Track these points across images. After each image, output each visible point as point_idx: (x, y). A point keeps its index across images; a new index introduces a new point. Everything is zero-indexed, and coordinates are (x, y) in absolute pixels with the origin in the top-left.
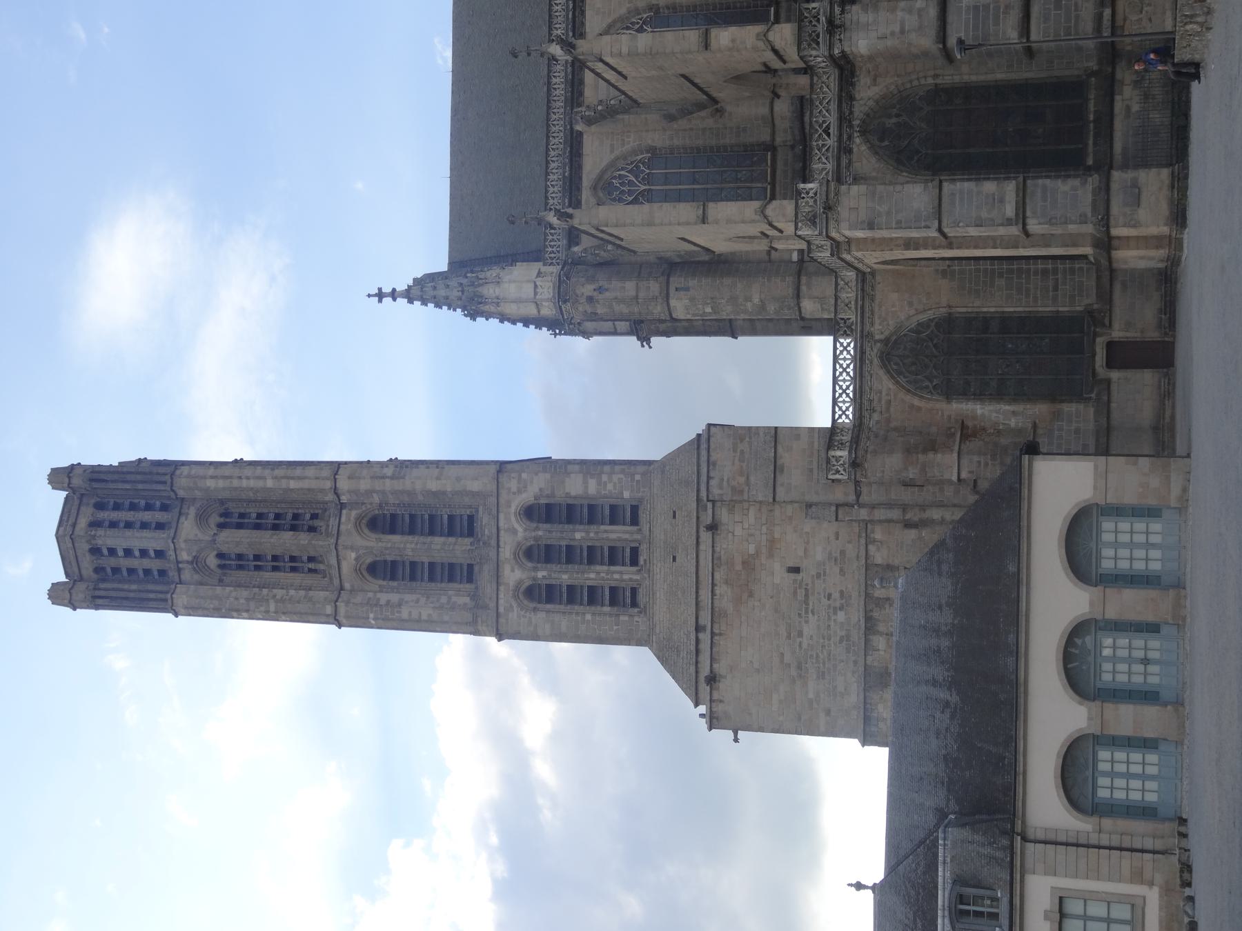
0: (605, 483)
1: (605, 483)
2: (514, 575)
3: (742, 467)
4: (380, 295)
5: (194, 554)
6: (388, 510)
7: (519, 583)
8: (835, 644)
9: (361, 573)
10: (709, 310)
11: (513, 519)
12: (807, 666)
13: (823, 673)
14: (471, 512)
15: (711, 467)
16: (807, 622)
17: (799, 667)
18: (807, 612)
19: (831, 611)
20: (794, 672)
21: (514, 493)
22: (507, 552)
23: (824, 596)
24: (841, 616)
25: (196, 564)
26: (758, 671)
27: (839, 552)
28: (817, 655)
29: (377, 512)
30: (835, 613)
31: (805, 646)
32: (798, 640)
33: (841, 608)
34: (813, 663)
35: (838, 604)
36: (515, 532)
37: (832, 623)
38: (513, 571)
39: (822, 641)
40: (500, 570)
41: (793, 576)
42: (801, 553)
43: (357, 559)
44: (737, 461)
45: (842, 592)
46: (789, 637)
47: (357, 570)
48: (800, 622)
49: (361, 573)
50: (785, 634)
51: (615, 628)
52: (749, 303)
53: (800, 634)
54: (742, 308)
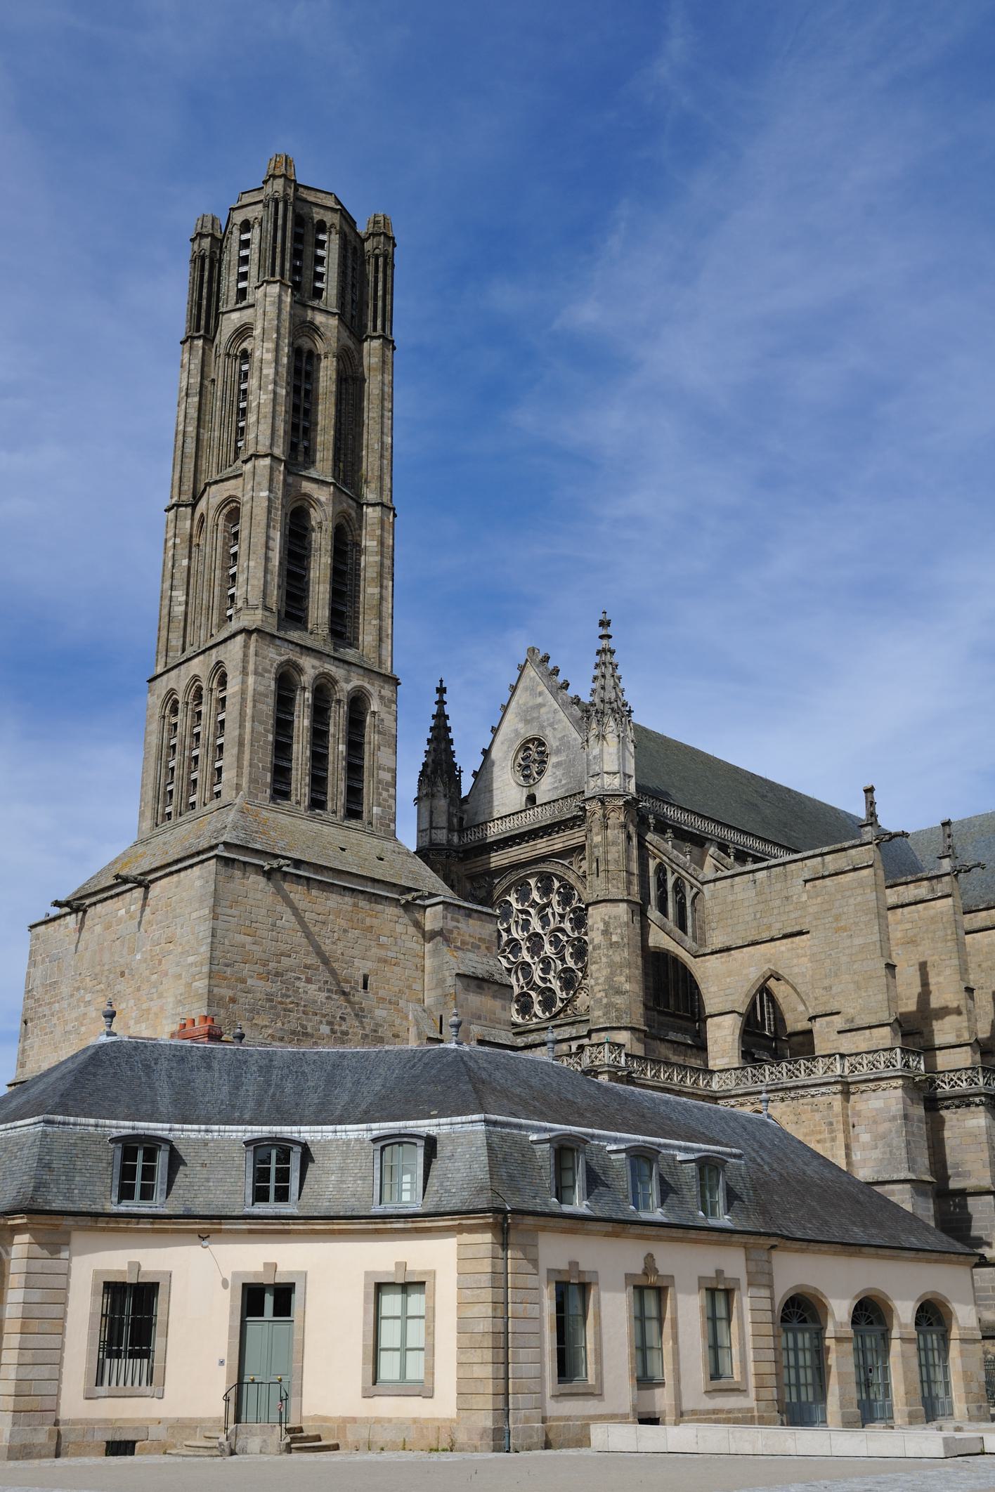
0: (388, 791)
1: (388, 791)
2: (310, 667)
3: (468, 944)
4: (604, 624)
5: (322, 329)
6: (352, 551)
7: (300, 670)
8: (299, 1019)
9: (300, 499)
10: (615, 938)
11: (359, 683)
12: (279, 983)
13: (272, 1001)
14: (349, 638)
15: (467, 912)
16: (320, 989)
17: (277, 974)
18: (329, 991)
19: (330, 1019)
20: (272, 965)
21: (380, 692)
22: (331, 668)
23: (342, 1013)
24: (325, 1029)
25: (308, 326)
26: (274, 925)
27: (383, 1035)
28: (290, 997)
29: (350, 538)
30: (330, 1023)
31: (297, 983)
32: (303, 977)
33: (333, 1031)
34: (281, 990)
35: (336, 1027)
36: (348, 681)
37: (318, 1018)
38: (313, 667)
39: (303, 1003)
40: (314, 654)
41: (361, 981)
42: (382, 993)
43: (318, 501)
44: (472, 940)
45: (345, 1033)
46: (306, 967)
47: (307, 497)
48: (319, 981)
49: (300, 499)
50: (309, 962)
51: (260, 765)
52: (624, 979)
53: (309, 981)
54: (618, 971)
